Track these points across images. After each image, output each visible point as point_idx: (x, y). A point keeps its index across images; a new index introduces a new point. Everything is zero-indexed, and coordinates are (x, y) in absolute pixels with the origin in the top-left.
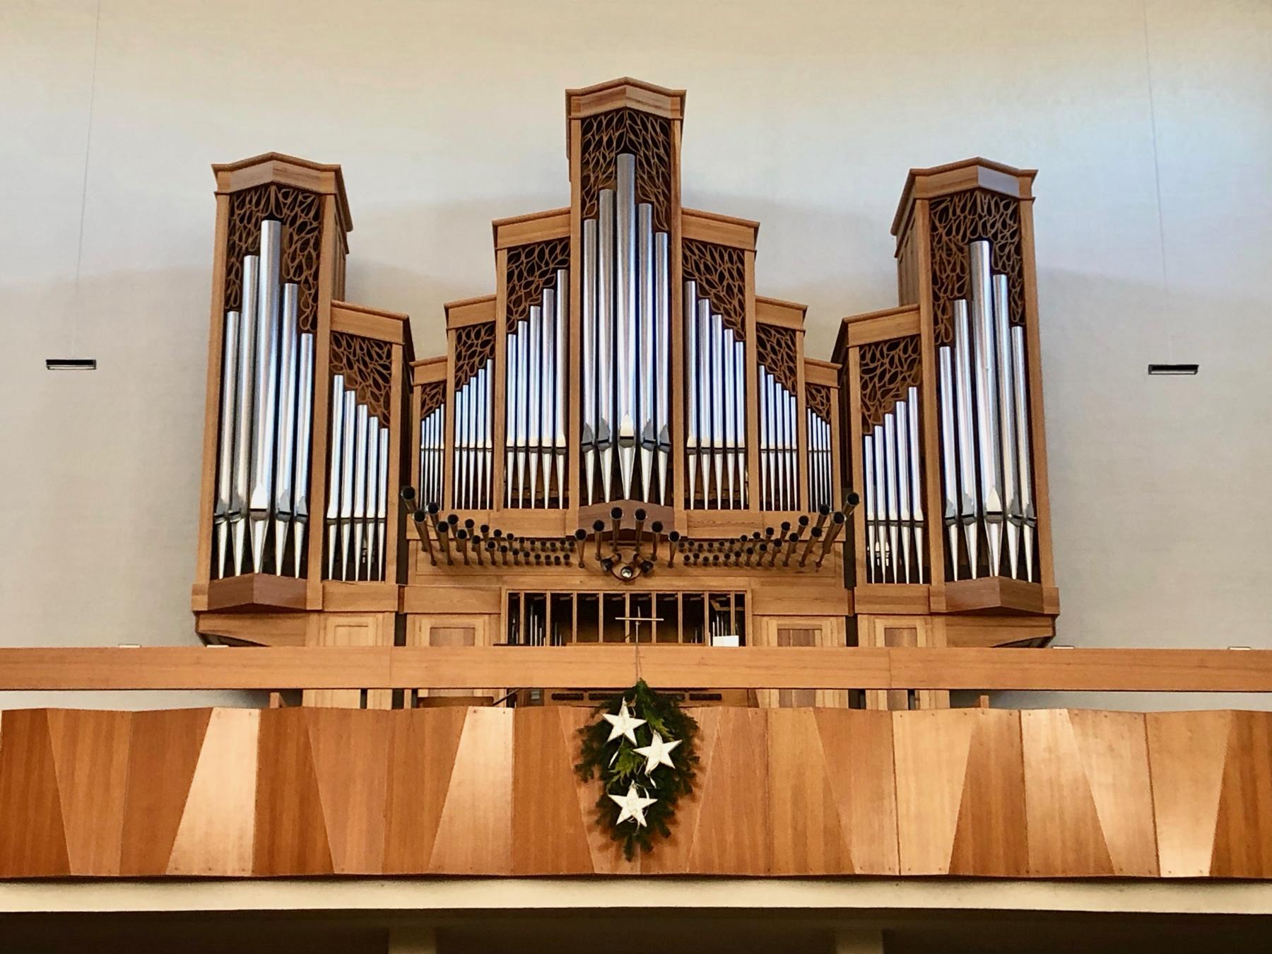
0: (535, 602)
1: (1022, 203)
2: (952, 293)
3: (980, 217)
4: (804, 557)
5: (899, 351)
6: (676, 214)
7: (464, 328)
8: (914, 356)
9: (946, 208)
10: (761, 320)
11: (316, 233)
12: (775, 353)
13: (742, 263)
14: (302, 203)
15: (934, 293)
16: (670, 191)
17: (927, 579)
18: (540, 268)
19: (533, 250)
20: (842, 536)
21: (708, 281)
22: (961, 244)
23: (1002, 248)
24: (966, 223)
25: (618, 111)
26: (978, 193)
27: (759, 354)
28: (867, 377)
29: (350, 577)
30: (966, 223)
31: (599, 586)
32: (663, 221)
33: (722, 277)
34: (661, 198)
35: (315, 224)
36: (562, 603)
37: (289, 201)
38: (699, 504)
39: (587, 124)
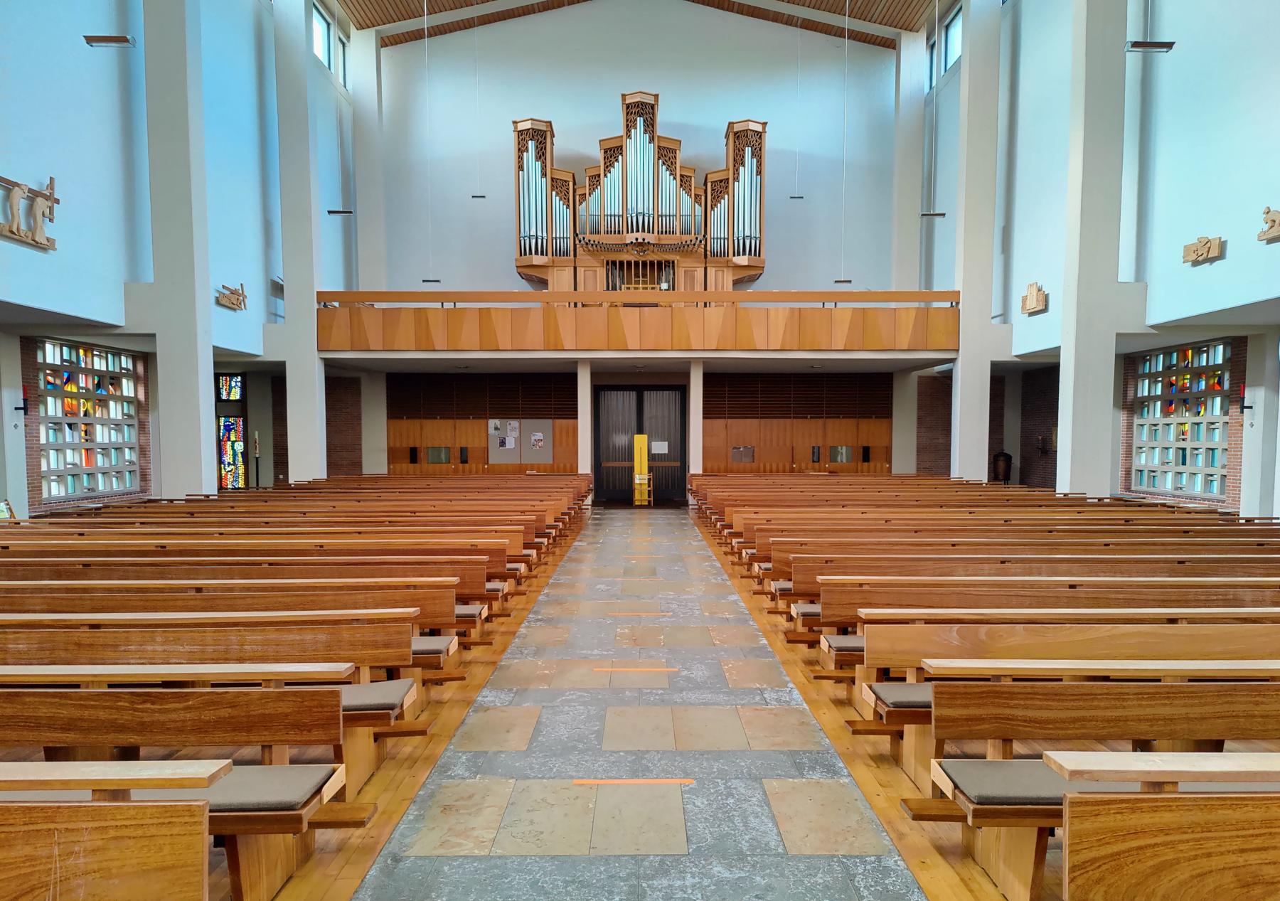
0: (614, 263)
30: (745, 141)
31: (632, 259)
36: (621, 263)
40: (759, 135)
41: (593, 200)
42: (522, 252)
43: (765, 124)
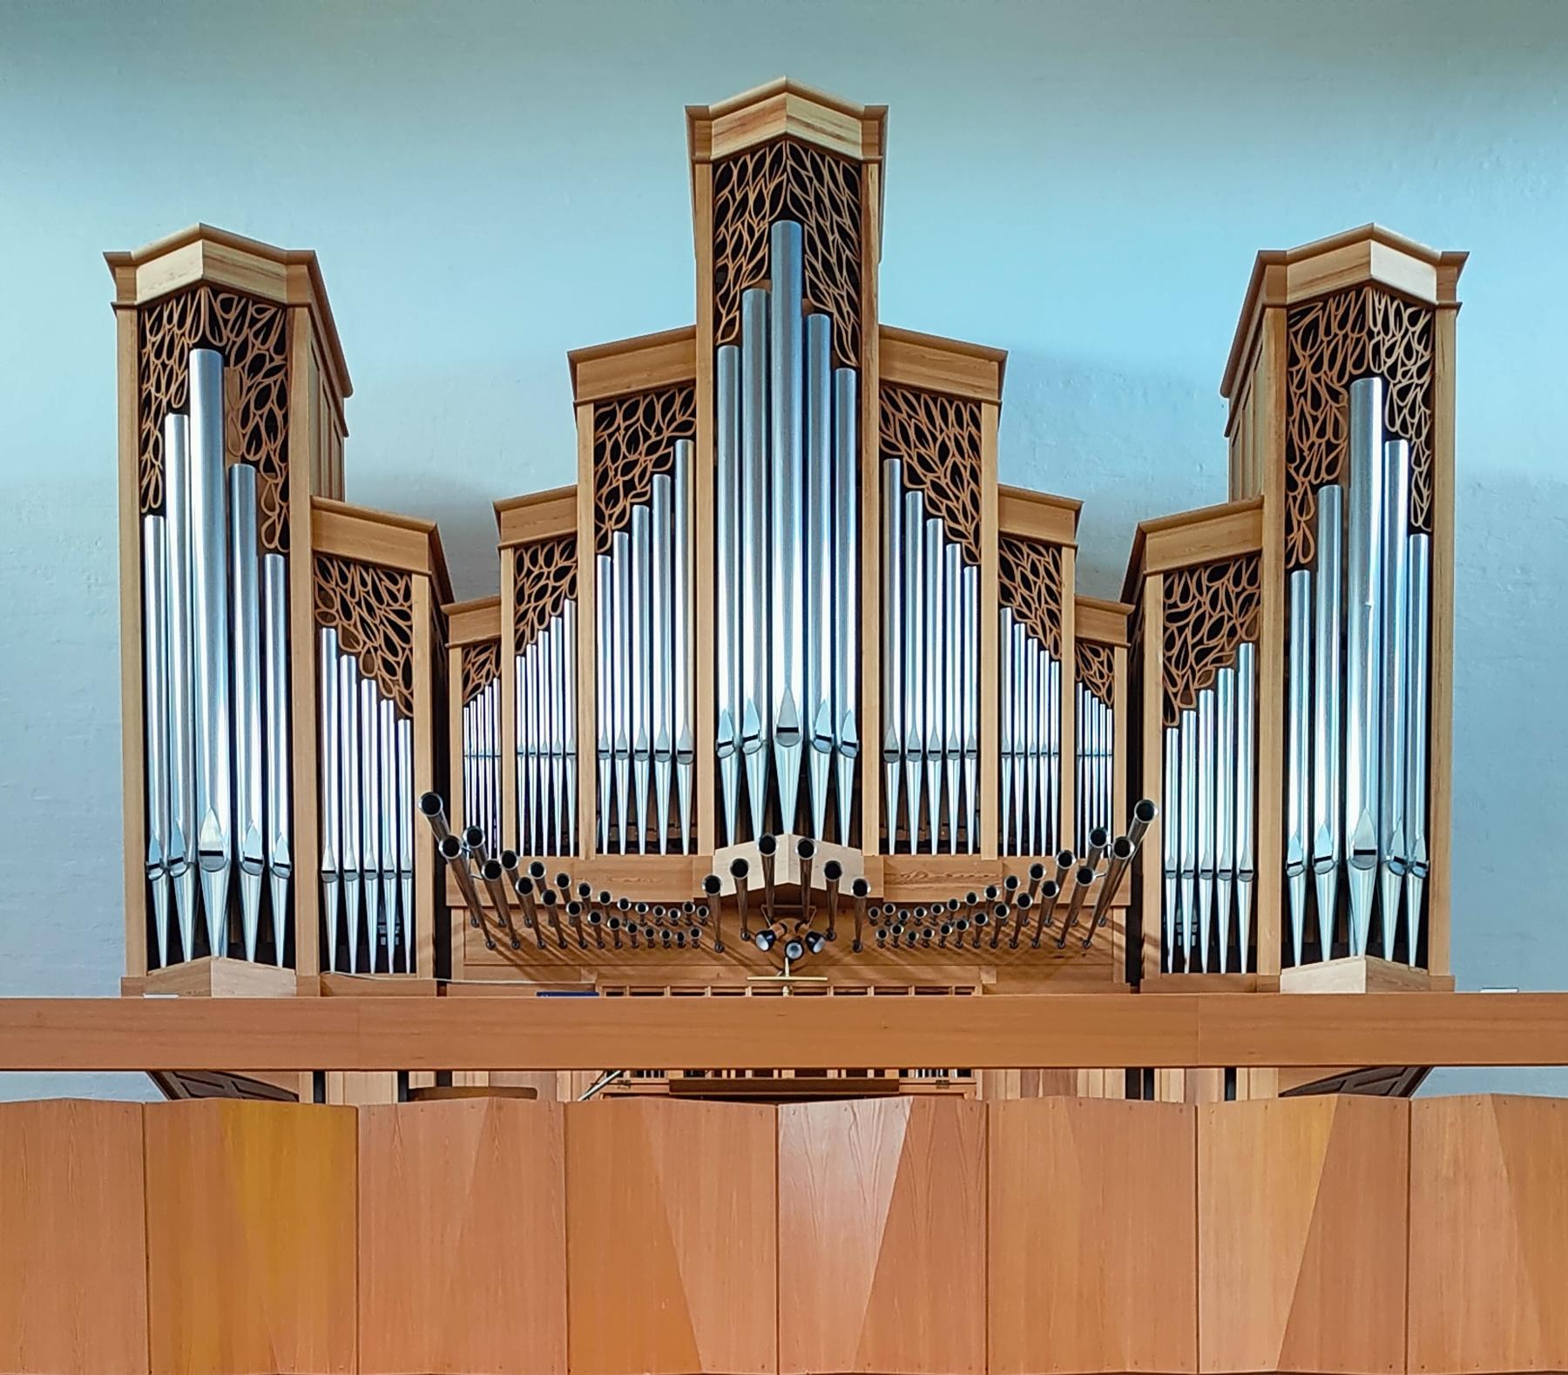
1: (1438, 313)
2: (1316, 477)
3: (1371, 335)
4: (1065, 931)
5: (1226, 582)
6: (869, 335)
7: (526, 546)
8: (1250, 590)
9: (1314, 324)
10: (1010, 529)
11: (280, 376)
12: (1028, 588)
13: (976, 423)
14: (254, 321)
15: (1289, 476)
16: (859, 294)
17: (1252, 967)
18: (647, 437)
19: (637, 404)
20: (1123, 897)
21: (921, 458)
22: (1337, 386)
23: (1403, 393)
24: (1339, 352)
25: (771, 143)
26: (1370, 294)
27: (1003, 588)
28: (1174, 627)
29: (363, 966)
32: (848, 347)
33: (944, 453)
34: (846, 308)
35: (278, 360)
37: (232, 316)
38: (903, 847)
39: (722, 172)
40: (1427, 319)
41: (535, 671)
42: (163, 946)
43: (1450, 265)
